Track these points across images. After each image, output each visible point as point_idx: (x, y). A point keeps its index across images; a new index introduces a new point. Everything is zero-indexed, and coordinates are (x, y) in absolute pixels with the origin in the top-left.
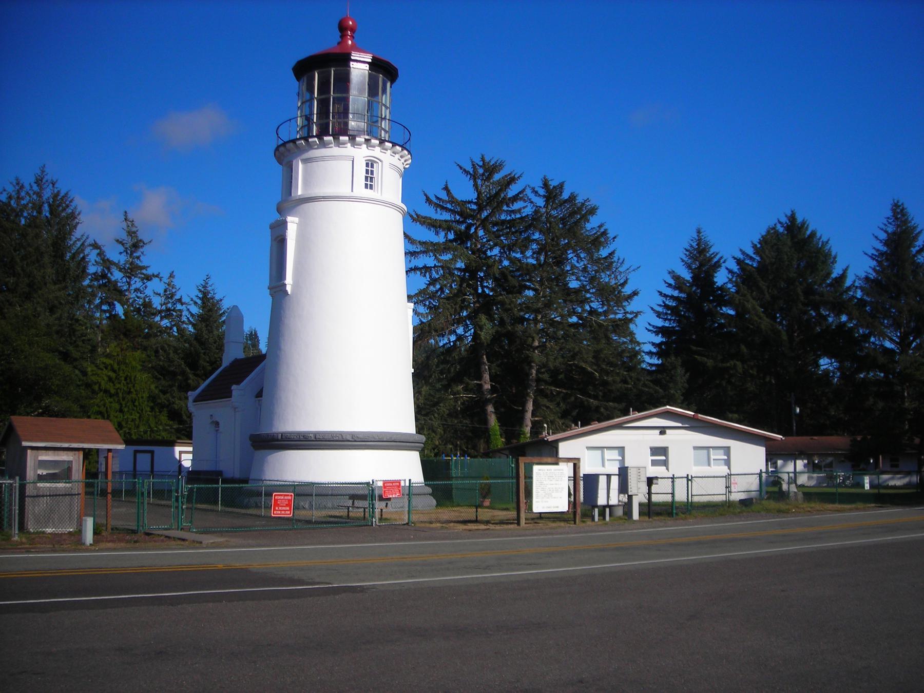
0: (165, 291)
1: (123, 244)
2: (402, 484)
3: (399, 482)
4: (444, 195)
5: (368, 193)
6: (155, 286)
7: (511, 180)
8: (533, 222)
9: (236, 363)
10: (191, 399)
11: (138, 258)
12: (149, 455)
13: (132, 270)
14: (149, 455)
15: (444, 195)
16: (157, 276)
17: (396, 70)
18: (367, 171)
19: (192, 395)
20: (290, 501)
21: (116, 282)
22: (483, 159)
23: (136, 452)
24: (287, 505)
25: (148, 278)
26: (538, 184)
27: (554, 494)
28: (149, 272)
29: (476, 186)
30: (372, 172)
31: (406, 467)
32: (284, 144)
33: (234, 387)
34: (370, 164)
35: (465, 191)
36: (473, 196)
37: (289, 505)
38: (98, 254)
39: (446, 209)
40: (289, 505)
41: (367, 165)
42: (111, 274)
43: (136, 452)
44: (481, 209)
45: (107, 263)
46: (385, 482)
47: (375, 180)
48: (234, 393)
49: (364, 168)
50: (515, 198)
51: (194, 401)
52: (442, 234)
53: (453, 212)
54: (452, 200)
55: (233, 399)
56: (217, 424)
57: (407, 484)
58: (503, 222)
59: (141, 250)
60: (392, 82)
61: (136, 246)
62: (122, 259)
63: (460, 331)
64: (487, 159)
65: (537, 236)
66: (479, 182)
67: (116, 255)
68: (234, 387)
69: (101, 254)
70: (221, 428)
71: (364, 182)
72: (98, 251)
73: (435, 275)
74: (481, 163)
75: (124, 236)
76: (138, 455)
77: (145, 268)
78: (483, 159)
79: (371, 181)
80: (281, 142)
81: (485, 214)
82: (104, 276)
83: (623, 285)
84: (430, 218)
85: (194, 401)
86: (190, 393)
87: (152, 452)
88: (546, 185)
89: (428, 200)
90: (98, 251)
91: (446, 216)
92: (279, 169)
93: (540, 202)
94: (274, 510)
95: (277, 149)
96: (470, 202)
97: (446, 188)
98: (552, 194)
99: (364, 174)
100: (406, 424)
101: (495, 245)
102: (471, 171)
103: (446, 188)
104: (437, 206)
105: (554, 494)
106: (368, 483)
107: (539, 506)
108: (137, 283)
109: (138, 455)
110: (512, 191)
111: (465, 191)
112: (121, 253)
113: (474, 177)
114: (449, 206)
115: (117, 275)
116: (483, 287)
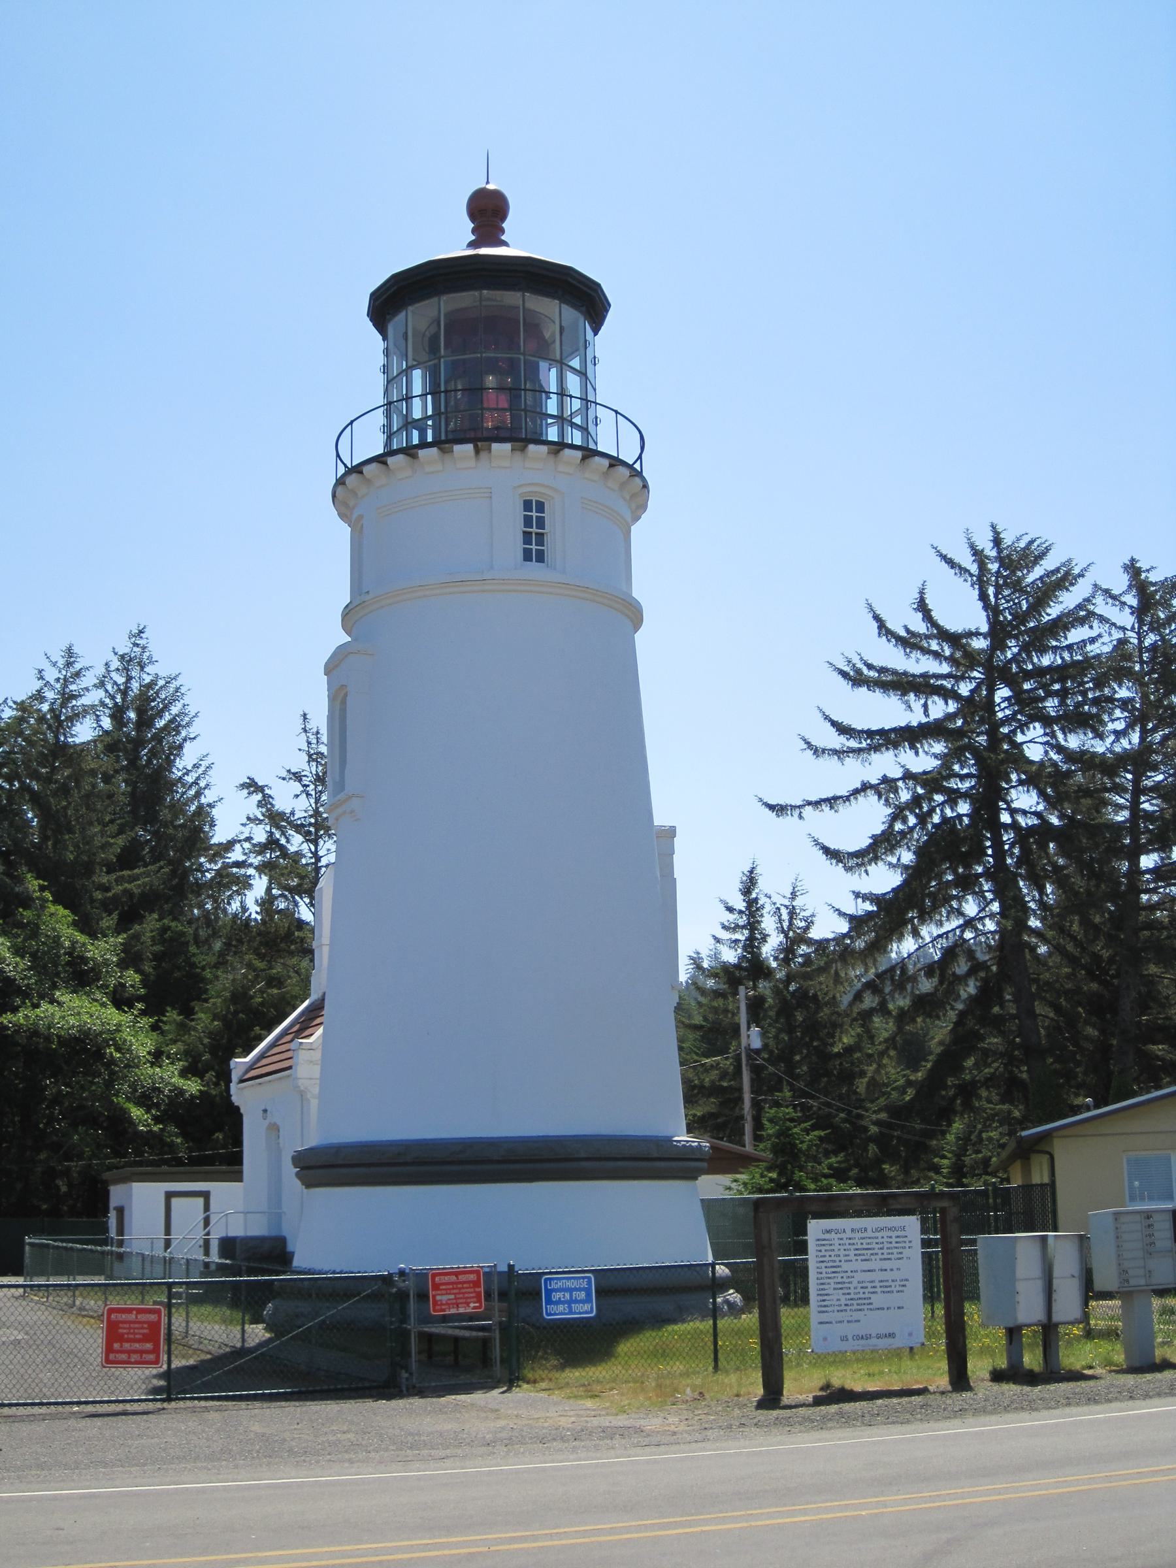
1: (300, 781)
4: (921, 627)
8: (1117, 666)
12: (200, 1201)
14: (200, 1201)
15: (921, 627)
17: (594, 287)
18: (528, 521)
23: (169, 1195)
26: (1119, 582)
29: (983, 597)
38: (260, 804)
39: (926, 651)
41: (527, 505)
42: (288, 842)
43: (169, 1195)
45: (275, 818)
49: (520, 513)
54: (944, 635)
58: (1050, 669)
63: (971, 907)
64: (1008, 539)
65: (1123, 693)
66: (991, 591)
69: (266, 802)
72: (259, 797)
76: (175, 1201)
78: (997, 541)
79: (540, 542)
82: (272, 843)
87: (206, 1195)
88: (1139, 583)
90: (259, 797)
93: (1127, 619)
95: (334, 496)
96: (970, 634)
97: (922, 607)
101: (1033, 718)
102: (974, 569)
104: (900, 640)
105: (878, 1300)
109: (175, 1201)
110: (1068, 600)
112: (297, 796)
114: (934, 645)
115: (296, 843)
116: (1013, 812)
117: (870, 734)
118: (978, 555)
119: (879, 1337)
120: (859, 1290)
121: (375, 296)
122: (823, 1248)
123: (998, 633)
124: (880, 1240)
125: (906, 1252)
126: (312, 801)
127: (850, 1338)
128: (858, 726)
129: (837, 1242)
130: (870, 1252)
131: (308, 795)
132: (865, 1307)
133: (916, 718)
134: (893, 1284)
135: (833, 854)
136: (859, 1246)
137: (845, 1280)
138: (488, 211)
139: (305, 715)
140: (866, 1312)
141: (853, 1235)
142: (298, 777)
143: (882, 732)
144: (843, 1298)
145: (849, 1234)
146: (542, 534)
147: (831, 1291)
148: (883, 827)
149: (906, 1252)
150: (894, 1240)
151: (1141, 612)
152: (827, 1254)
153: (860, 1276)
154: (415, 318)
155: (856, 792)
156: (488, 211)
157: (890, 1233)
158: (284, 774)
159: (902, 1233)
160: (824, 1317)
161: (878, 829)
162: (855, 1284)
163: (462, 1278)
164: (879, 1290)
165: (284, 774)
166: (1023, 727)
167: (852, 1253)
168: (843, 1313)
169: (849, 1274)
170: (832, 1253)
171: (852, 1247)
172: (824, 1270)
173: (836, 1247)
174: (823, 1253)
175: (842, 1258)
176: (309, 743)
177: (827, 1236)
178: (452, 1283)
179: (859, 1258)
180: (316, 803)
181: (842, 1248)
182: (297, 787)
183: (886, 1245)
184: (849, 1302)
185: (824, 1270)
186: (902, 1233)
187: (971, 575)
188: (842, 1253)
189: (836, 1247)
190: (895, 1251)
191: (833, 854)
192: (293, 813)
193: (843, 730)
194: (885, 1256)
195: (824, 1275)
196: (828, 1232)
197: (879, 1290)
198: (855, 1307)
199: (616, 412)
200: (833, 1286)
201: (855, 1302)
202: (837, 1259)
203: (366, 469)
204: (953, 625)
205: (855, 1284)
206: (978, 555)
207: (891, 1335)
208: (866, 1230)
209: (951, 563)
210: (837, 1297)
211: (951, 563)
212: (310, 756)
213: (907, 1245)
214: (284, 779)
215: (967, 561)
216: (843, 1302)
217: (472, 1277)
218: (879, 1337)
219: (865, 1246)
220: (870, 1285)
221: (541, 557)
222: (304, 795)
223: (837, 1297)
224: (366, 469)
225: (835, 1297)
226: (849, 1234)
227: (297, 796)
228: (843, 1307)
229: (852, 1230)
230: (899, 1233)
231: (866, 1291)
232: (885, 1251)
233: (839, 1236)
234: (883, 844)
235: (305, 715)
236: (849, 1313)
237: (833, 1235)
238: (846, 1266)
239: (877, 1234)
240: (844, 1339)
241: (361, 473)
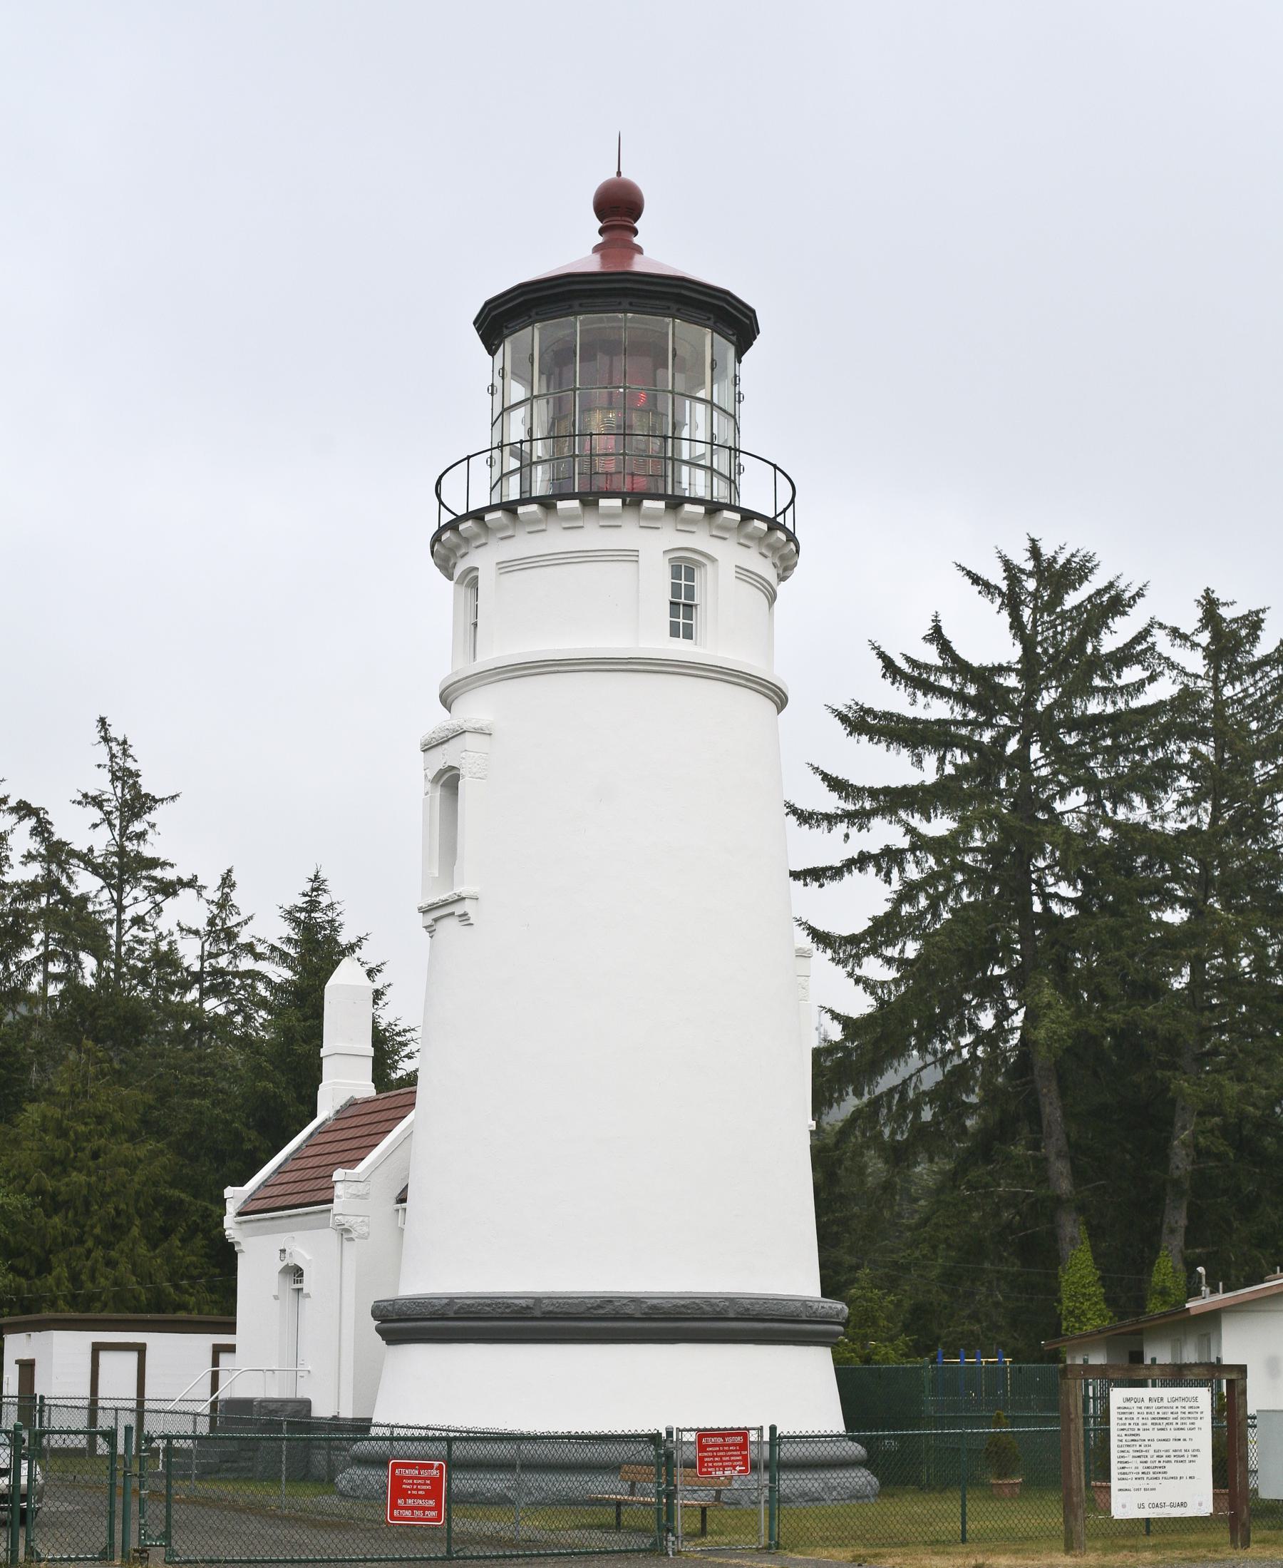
0: (211, 922)
1: (101, 807)
2: (753, 1436)
3: (743, 1433)
4: (930, 655)
5: (680, 649)
6: (187, 910)
7: (1113, 604)
9: (352, 1108)
10: (231, 1208)
11: (141, 836)
12: (133, 1357)
13: (126, 868)
14: (133, 1357)
15: (930, 655)
16: (191, 883)
18: (676, 589)
19: (235, 1196)
20: (436, 1482)
21: (84, 899)
22: (1035, 552)
23: (97, 1348)
24: (428, 1496)
25: (168, 889)
27: (1172, 1469)
28: (168, 874)
29: (1017, 625)
30: (690, 592)
31: (795, 1394)
32: (453, 526)
33: (338, 1174)
34: (684, 570)
35: (989, 640)
36: (1011, 652)
37: (434, 1493)
38: (34, 832)
40: (434, 1493)
41: (676, 573)
42: (70, 880)
44: (1033, 687)
45: (57, 853)
46: (703, 1434)
47: (698, 614)
48: (339, 1190)
50: (1123, 657)
51: (240, 1214)
52: (930, 760)
53: (960, 697)
54: (959, 666)
55: (337, 1206)
56: (296, 1273)
57: (766, 1437)
59: (147, 817)
60: (741, 350)
61: (137, 804)
62: (101, 841)
64: (1047, 551)
66: (1026, 614)
67: (84, 831)
68: (338, 1174)
69: (42, 829)
70: (308, 1284)
71: (666, 619)
73: (913, 873)
74: (1029, 566)
75: (101, 783)
76: (104, 1357)
77: (154, 863)
78: (1035, 552)
79: (689, 616)
80: (447, 517)
81: (1048, 697)
82: (51, 885)
83: (97, 802)
84: (900, 719)
85: (240, 1214)
86: (229, 1192)
87: (141, 1349)
89: (890, 667)
91: (939, 709)
92: (445, 588)
93: (1195, 662)
94: (394, 1506)
95: (436, 538)
96: (1001, 670)
98: (1227, 639)
99: (668, 596)
100: (796, 1275)
101: (1075, 783)
102: (1004, 586)
103: (936, 635)
106: (654, 1438)
107: (1128, 1500)
108: (137, 900)
109: (104, 1357)
111: (989, 640)
112: (95, 826)
113: (1012, 602)
115: (85, 883)
116: (1046, 898)
117: (873, 793)
118: (1008, 566)
119: (1172, 1505)
121: (490, 306)
123: (1029, 667)
124: (1175, 1410)
126: (117, 832)
128: (858, 781)
131: (111, 825)
133: (929, 775)
135: (822, 938)
138: (619, 208)
139: (102, 721)
141: (1150, 1404)
142: (97, 802)
143: (887, 791)
145: (1147, 1403)
146: (691, 606)
148: (887, 907)
150: (1187, 1410)
151: (1213, 656)
153: (1156, 1446)
154: (533, 337)
155: (849, 864)
156: (619, 208)
157: (1184, 1404)
158: (80, 798)
160: (1123, 1485)
161: (883, 908)
162: (1151, 1449)
163: (729, 1440)
164: (1173, 1459)
165: (80, 798)
166: (1063, 792)
172: (1124, 1438)
173: (1135, 1416)
175: (1140, 1427)
176: (113, 756)
177: (1127, 1404)
178: (719, 1446)
180: (121, 835)
182: (95, 814)
183: (1180, 1415)
185: (1124, 1438)
186: (1195, 1404)
187: (1001, 593)
189: (1135, 1416)
190: (1188, 1421)
191: (822, 938)
192: (91, 850)
193: (836, 785)
196: (1128, 1400)
197: (1173, 1459)
198: (1152, 1475)
199: (775, 467)
200: (1132, 1454)
201: (1151, 1471)
203: (488, 517)
204: (976, 656)
205: (1151, 1453)
206: (1008, 566)
207: (1183, 1505)
209: (976, 579)
210: (1135, 1465)
211: (976, 579)
212: (113, 773)
213: (1199, 1416)
214: (80, 803)
215: (998, 578)
216: (1141, 1470)
217: (739, 1439)
218: (1172, 1505)
221: (688, 635)
222: (106, 825)
223: (1135, 1465)
224: (488, 517)
226: (1147, 1403)
227: (95, 826)
232: (1179, 1421)
234: (884, 930)
235: (102, 721)
236: (1146, 1481)
237: (1132, 1404)
238: (1144, 1435)
240: (1141, 1506)
241: (483, 519)
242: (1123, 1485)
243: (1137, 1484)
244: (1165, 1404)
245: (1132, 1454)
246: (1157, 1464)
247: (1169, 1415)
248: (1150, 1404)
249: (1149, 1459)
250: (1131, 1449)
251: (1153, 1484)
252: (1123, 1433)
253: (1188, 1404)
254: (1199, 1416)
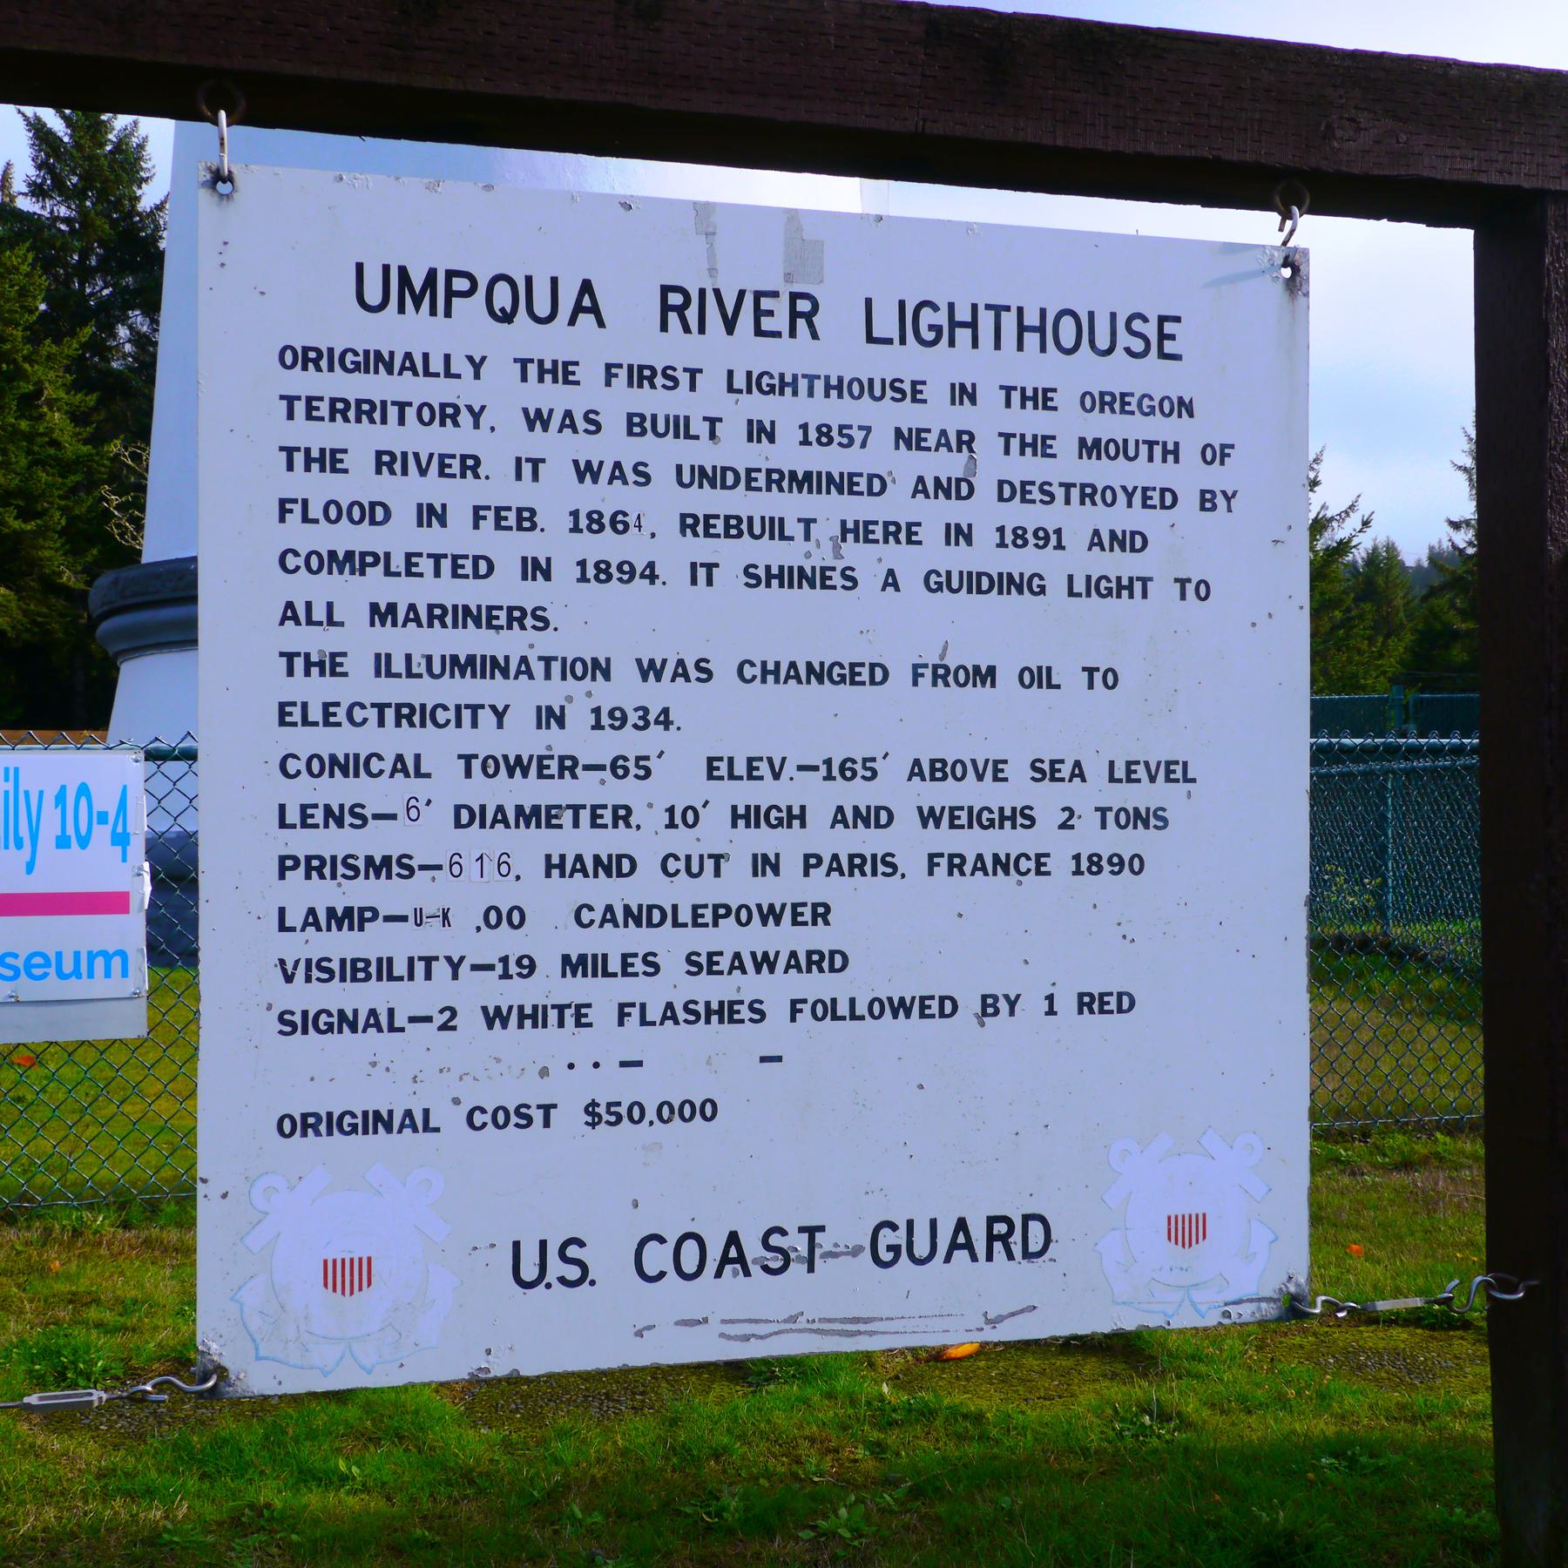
27: (894, 930)
105: (894, 930)
119: (889, 1247)
120: (714, 833)
122: (360, 441)
124: (938, 414)
125: (1177, 538)
127: (608, 1257)
129: (505, 396)
130: (831, 509)
132: (775, 989)
134: (1048, 800)
136: (735, 451)
137: (577, 739)
140: (776, 1032)
141: (674, 348)
144: (551, 902)
145: (633, 332)
147: (430, 837)
149: (1177, 538)
152: (404, 493)
153: (719, 718)
159: (1150, 377)
160: (341, 1073)
162: (680, 778)
167: (661, 503)
168: (554, 1042)
169: (625, 689)
170: (458, 495)
171: (662, 454)
172: (360, 641)
174: (360, 483)
179: (733, 554)
181: (560, 449)
183: (993, 464)
184: (613, 942)
185: (360, 641)
186: (1150, 377)
188: (556, 495)
190: (1077, 521)
194: (983, 556)
195: (360, 685)
197: (907, 841)
200: (449, 786)
201: (670, 944)
202: (508, 548)
205: (680, 778)
208: (803, 311)
213: (1188, 477)
216: (550, 935)
218: (889, 1247)
219: (788, 454)
220: (821, 797)
225: (468, 896)
226: (633, 332)
228: (549, 987)
229: (675, 305)
230: (1119, 374)
231: (788, 844)
232: (984, 512)
233: (524, 337)
236: (607, 1038)
238: (584, 619)
239: (906, 361)
242: (341, 1073)
243: (511, 1065)
244: (838, 348)
245: (449, 786)
246: (738, 886)
247: (879, 456)
248: (674, 348)
249: (647, 842)
250: (438, 747)
251: (678, 1061)
252: (352, 594)
253: (1075, 374)
254: (1188, 477)
